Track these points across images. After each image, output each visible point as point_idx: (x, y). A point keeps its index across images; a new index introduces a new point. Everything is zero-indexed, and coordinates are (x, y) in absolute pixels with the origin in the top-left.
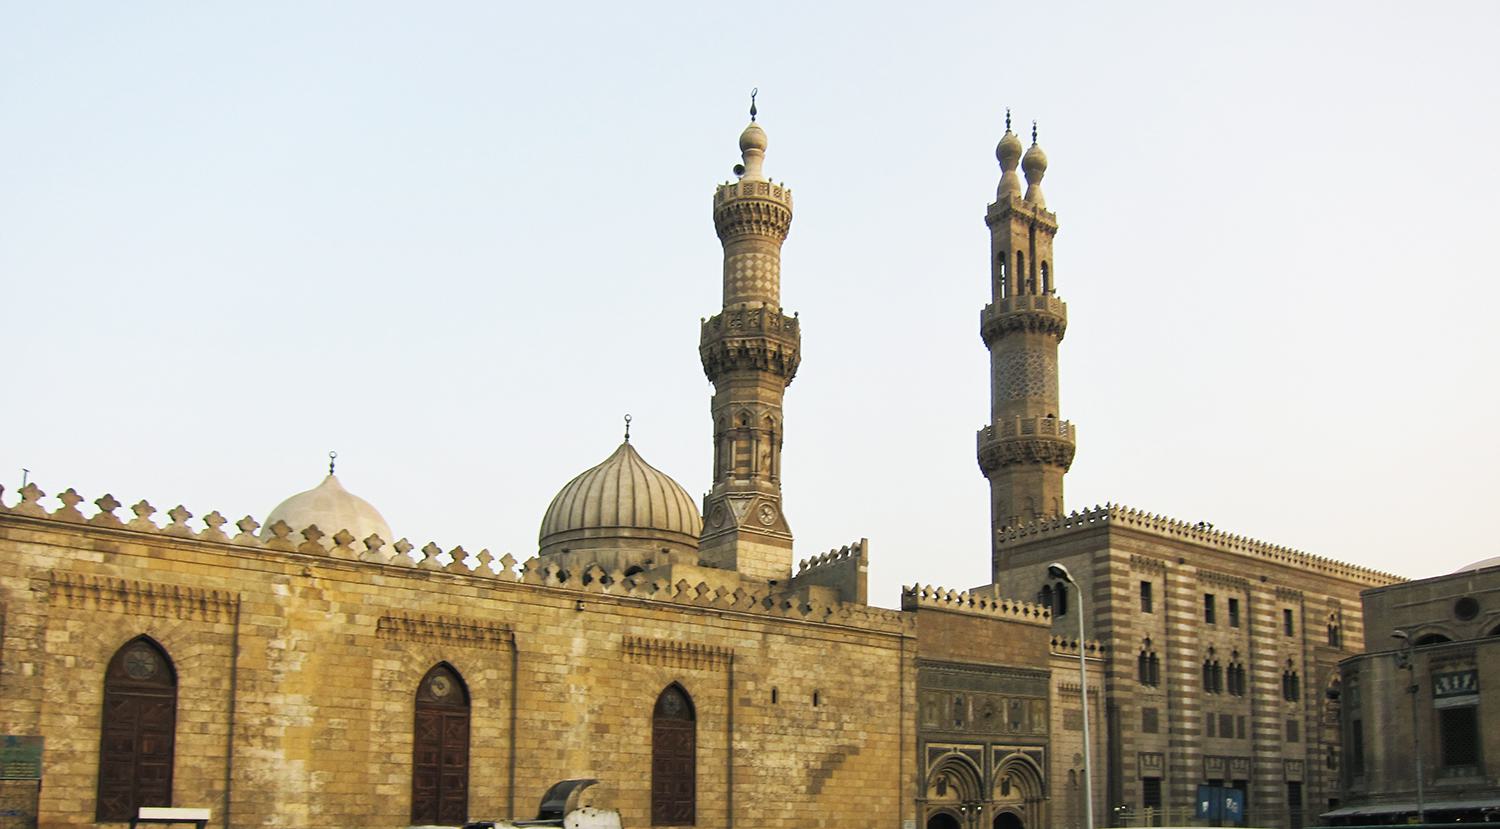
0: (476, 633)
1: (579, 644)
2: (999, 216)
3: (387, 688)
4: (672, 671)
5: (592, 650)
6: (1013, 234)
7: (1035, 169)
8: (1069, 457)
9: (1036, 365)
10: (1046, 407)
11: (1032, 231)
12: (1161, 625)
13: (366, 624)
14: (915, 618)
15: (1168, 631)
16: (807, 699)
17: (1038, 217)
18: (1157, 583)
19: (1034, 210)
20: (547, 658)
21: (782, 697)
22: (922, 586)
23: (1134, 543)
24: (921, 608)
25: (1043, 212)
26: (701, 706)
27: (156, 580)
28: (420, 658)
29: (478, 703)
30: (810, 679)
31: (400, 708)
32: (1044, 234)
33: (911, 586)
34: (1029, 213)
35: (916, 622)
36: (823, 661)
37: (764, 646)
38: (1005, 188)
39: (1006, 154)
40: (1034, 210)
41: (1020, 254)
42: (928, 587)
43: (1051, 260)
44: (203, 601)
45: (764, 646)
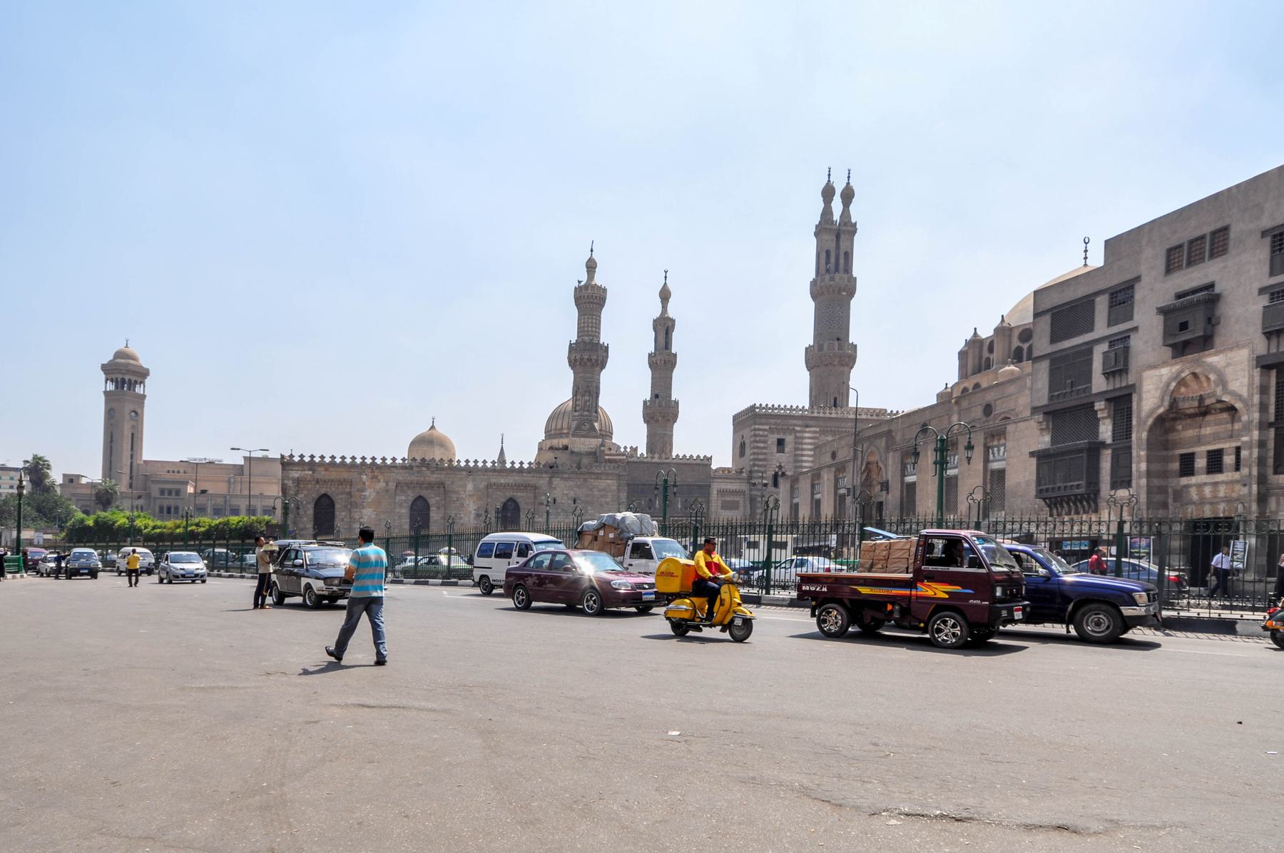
0: (431, 486)
1: (470, 487)
3: (401, 505)
4: (509, 494)
5: (475, 487)
7: (848, 195)
11: (838, 237)
12: (791, 459)
13: (392, 485)
15: (796, 461)
16: (571, 502)
18: (789, 439)
20: (457, 493)
21: (558, 501)
23: (773, 421)
26: (522, 506)
27: (327, 478)
28: (411, 496)
29: (433, 509)
30: (572, 494)
31: (405, 511)
36: (578, 487)
37: (550, 482)
38: (827, 212)
39: (828, 193)
44: (341, 482)
45: (550, 482)
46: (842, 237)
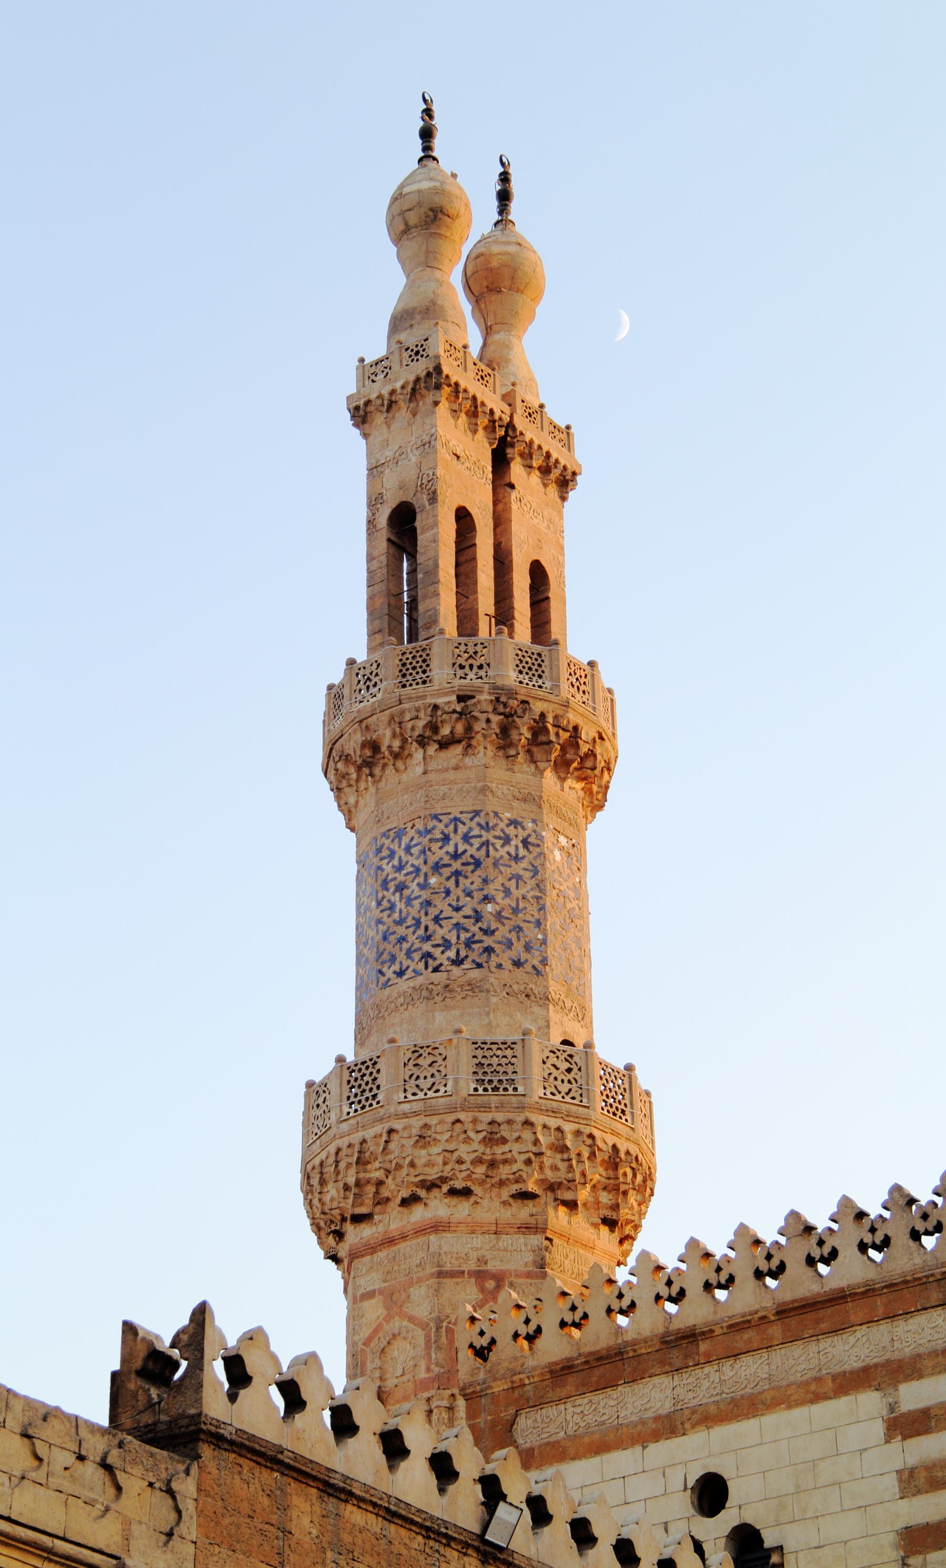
2: (402, 390)
6: (444, 454)
8: (633, 1198)
9: (518, 868)
10: (554, 1014)
14: (186, 1487)
17: (520, 423)
19: (508, 399)
22: (229, 1328)
24: (218, 1440)
25: (536, 413)
32: (535, 478)
33: (164, 1326)
34: (493, 401)
35: (189, 1507)
40: (508, 399)
41: (463, 516)
42: (255, 1337)
43: (561, 565)
46: (517, 470)
